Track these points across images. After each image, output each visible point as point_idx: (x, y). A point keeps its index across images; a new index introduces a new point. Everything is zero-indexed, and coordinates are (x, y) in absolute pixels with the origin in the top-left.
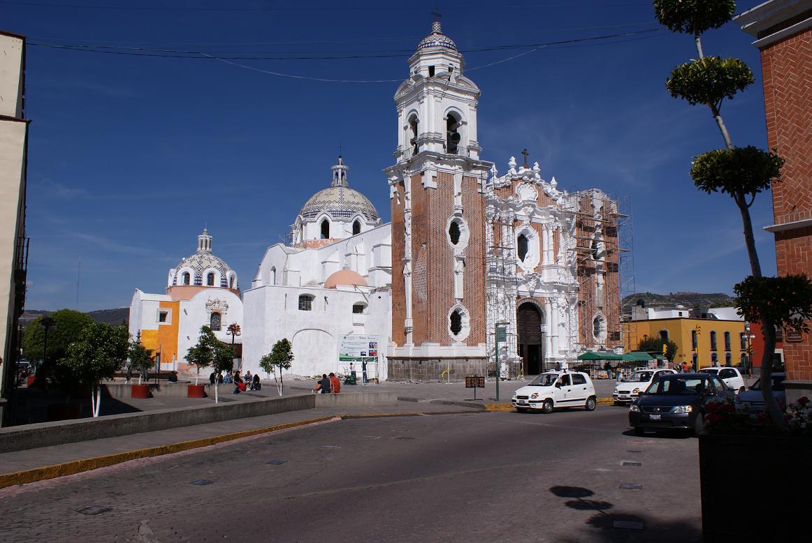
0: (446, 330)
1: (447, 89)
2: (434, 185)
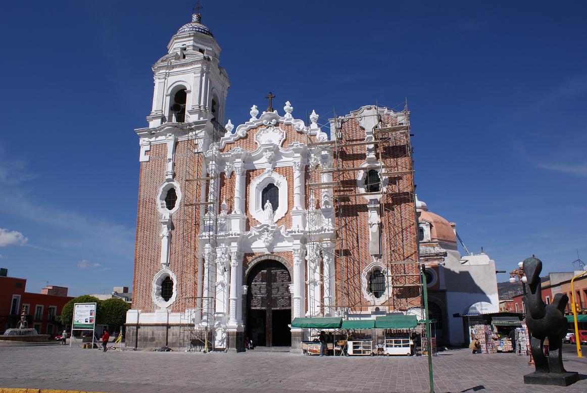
1: (173, 68)
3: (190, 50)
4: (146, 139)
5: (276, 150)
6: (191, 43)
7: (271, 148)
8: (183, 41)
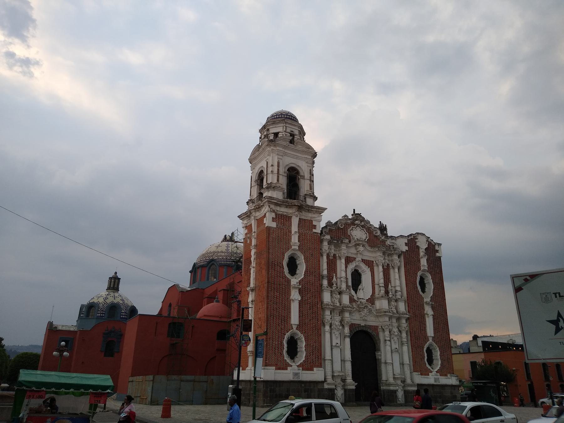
0: (281, 354)
2: (274, 225)
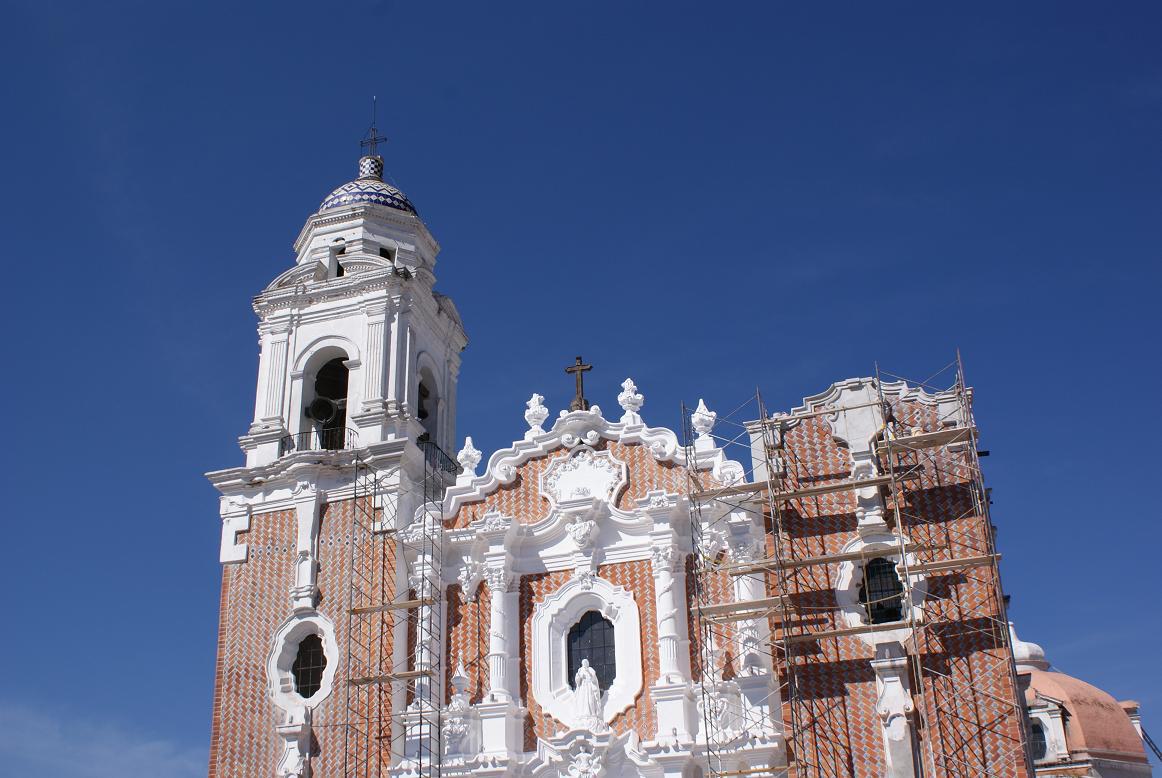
1: (311, 302)
3: (355, 252)
4: (239, 499)
5: (602, 518)
6: (359, 233)
7: (586, 511)
8: (335, 229)
